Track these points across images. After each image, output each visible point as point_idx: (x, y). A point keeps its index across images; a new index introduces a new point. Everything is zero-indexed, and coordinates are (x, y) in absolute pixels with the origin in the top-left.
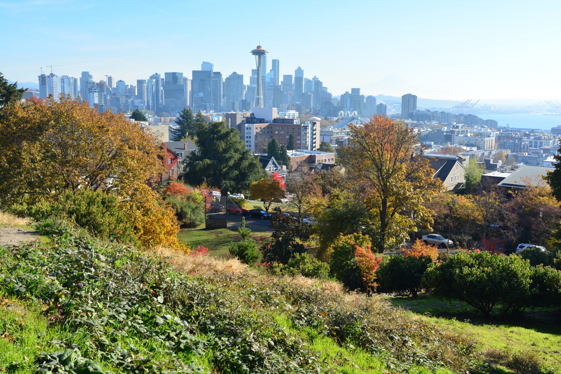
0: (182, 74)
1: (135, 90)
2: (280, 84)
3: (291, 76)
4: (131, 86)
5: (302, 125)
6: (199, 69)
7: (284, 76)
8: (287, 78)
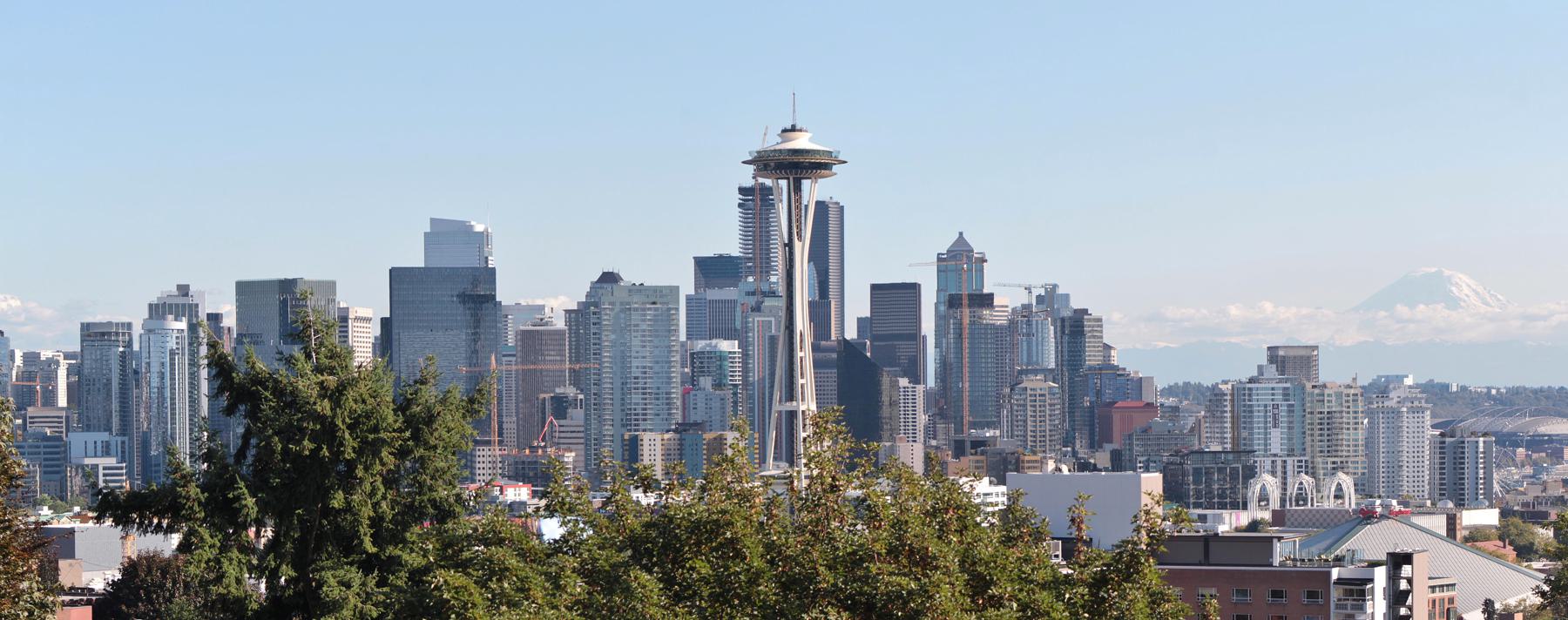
0: (331, 286)
1: (51, 377)
2: (851, 333)
3: (913, 288)
4: (31, 358)
5: (1335, 573)
6: (415, 258)
7: (874, 287)
8: (894, 299)
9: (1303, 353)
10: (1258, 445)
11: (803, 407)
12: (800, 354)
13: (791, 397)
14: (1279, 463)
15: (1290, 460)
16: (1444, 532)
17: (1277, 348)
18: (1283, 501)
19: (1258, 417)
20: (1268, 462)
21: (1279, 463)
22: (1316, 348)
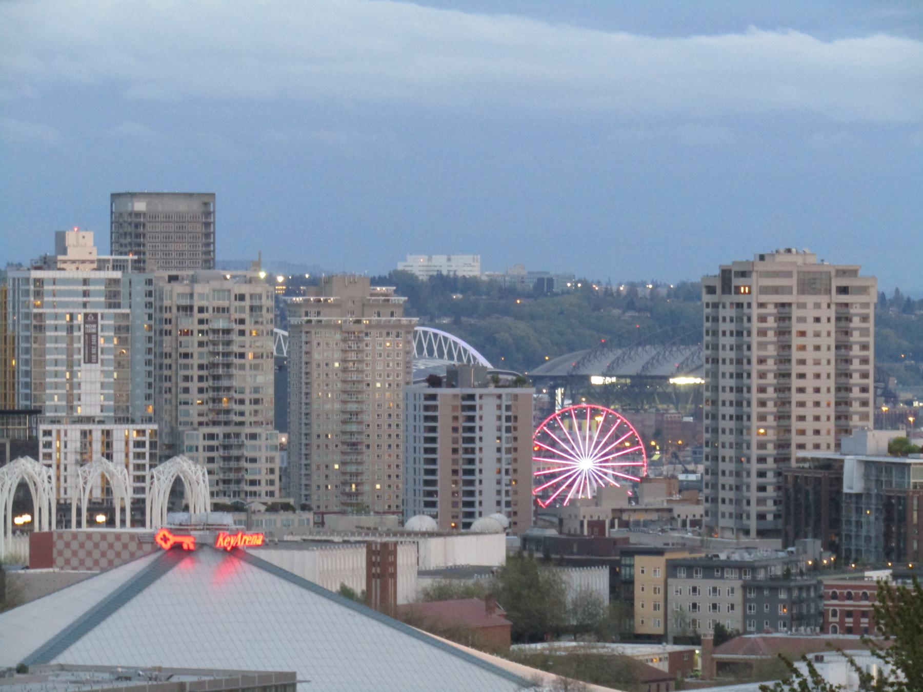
9: (182, 206)
10: (54, 400)
14: (97, 436)
17: (133, 195)
18: (63, 509)
19: (54, 346)
20: (74, 432)
21: (97, 431)
22: (207, 200)
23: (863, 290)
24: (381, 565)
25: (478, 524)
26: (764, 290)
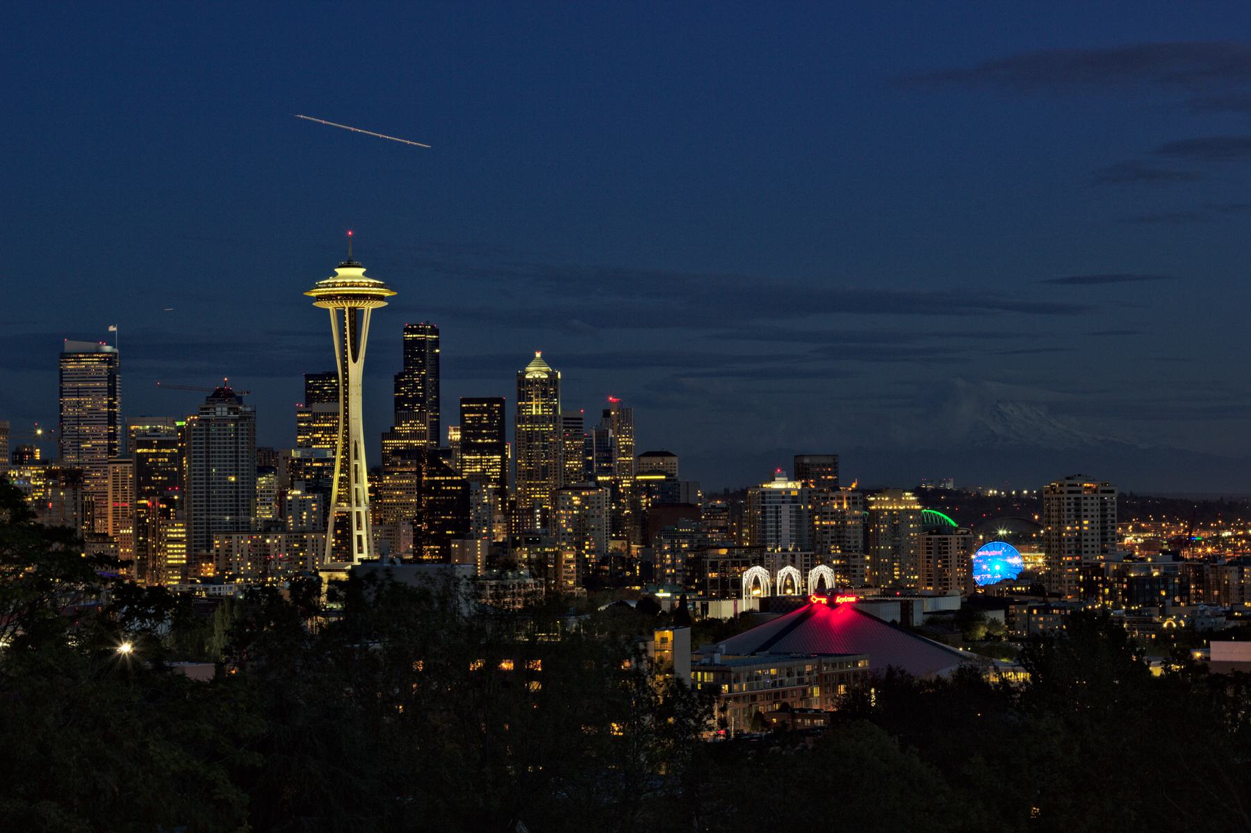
11: (358, 509)
12: (353, 462)
13: (349, 503)
14: (789, 557)
15: (798, 556)
16: (898, 620)
18: (774, 588)
22: (835, 456)
23: (1112, 492)
24: (906, 609)
25: (949, 592)
26: (1069, 492)
